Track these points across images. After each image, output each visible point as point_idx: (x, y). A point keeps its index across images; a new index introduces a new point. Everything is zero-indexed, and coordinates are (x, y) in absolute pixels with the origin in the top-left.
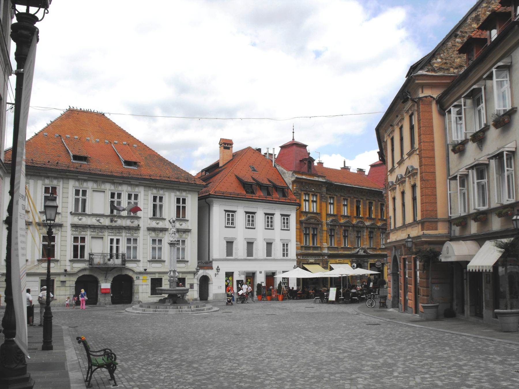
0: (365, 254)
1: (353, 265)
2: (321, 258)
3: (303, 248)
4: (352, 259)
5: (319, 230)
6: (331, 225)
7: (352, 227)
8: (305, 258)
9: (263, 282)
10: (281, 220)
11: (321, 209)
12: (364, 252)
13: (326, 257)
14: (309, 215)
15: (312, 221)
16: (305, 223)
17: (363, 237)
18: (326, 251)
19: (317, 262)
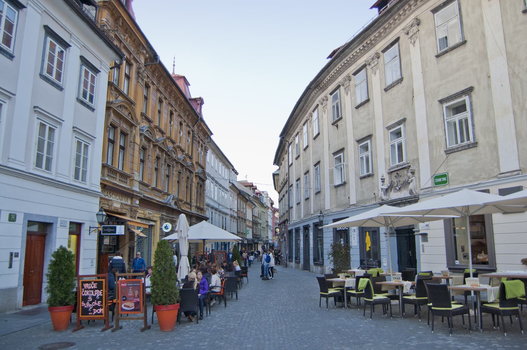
0: (175, 207)
1: (165, 225)
2: (129, 202)
3: (106, 171)
4: (162, 215)
5: (130, 138)
6: (146, 137)
7: (166, 154)
8: (107, 197)
9: (17, 255)
10: (80, 75)
11: (135, 98)
12: (176, 203)
13: (138, 202)
14: (120, 98)
15: (125, 113)
16: (115, 113)
17: (173, 177)
18: (136, 188)
19: (124, 211)
